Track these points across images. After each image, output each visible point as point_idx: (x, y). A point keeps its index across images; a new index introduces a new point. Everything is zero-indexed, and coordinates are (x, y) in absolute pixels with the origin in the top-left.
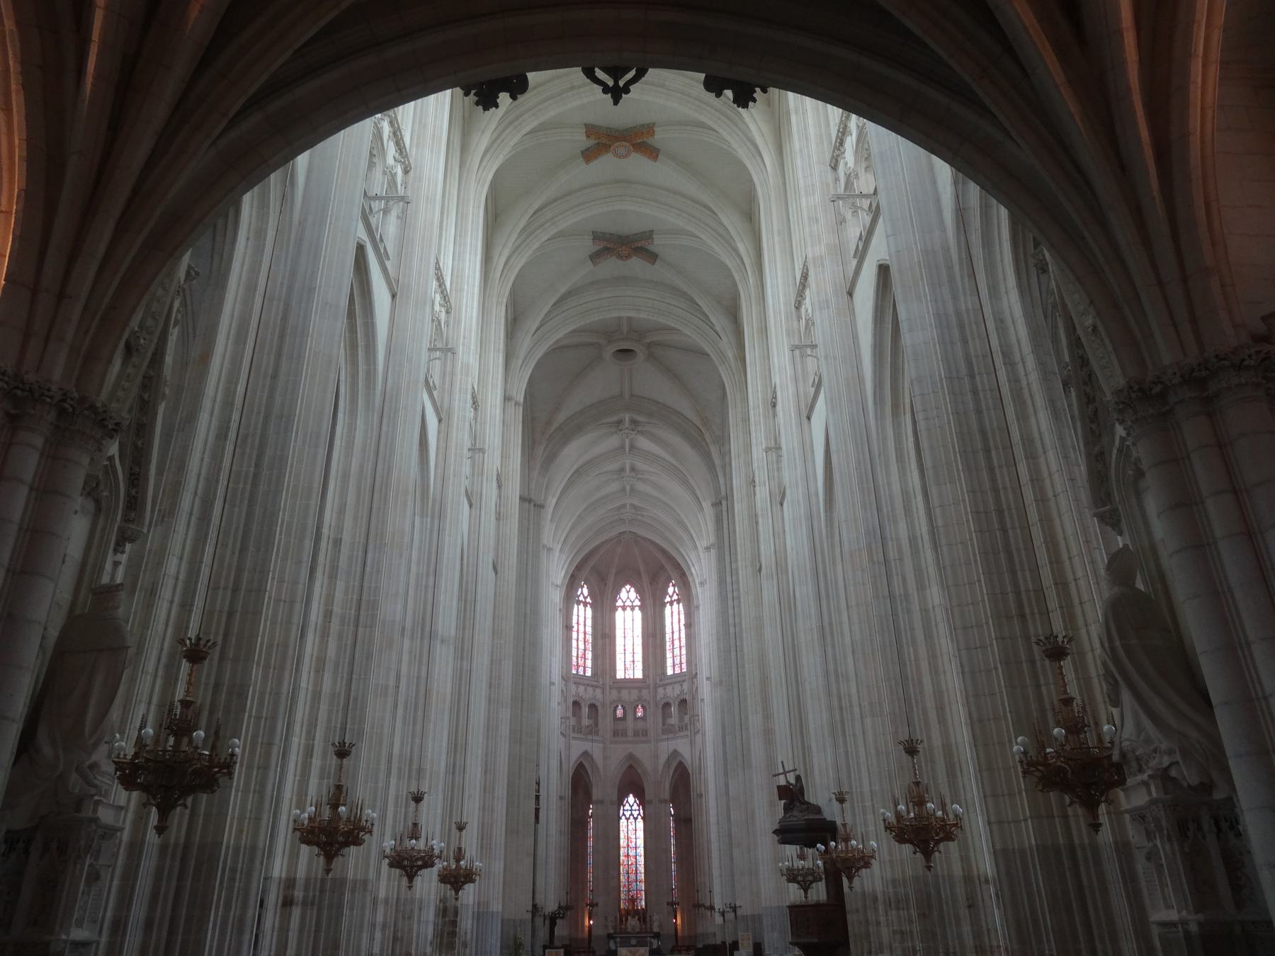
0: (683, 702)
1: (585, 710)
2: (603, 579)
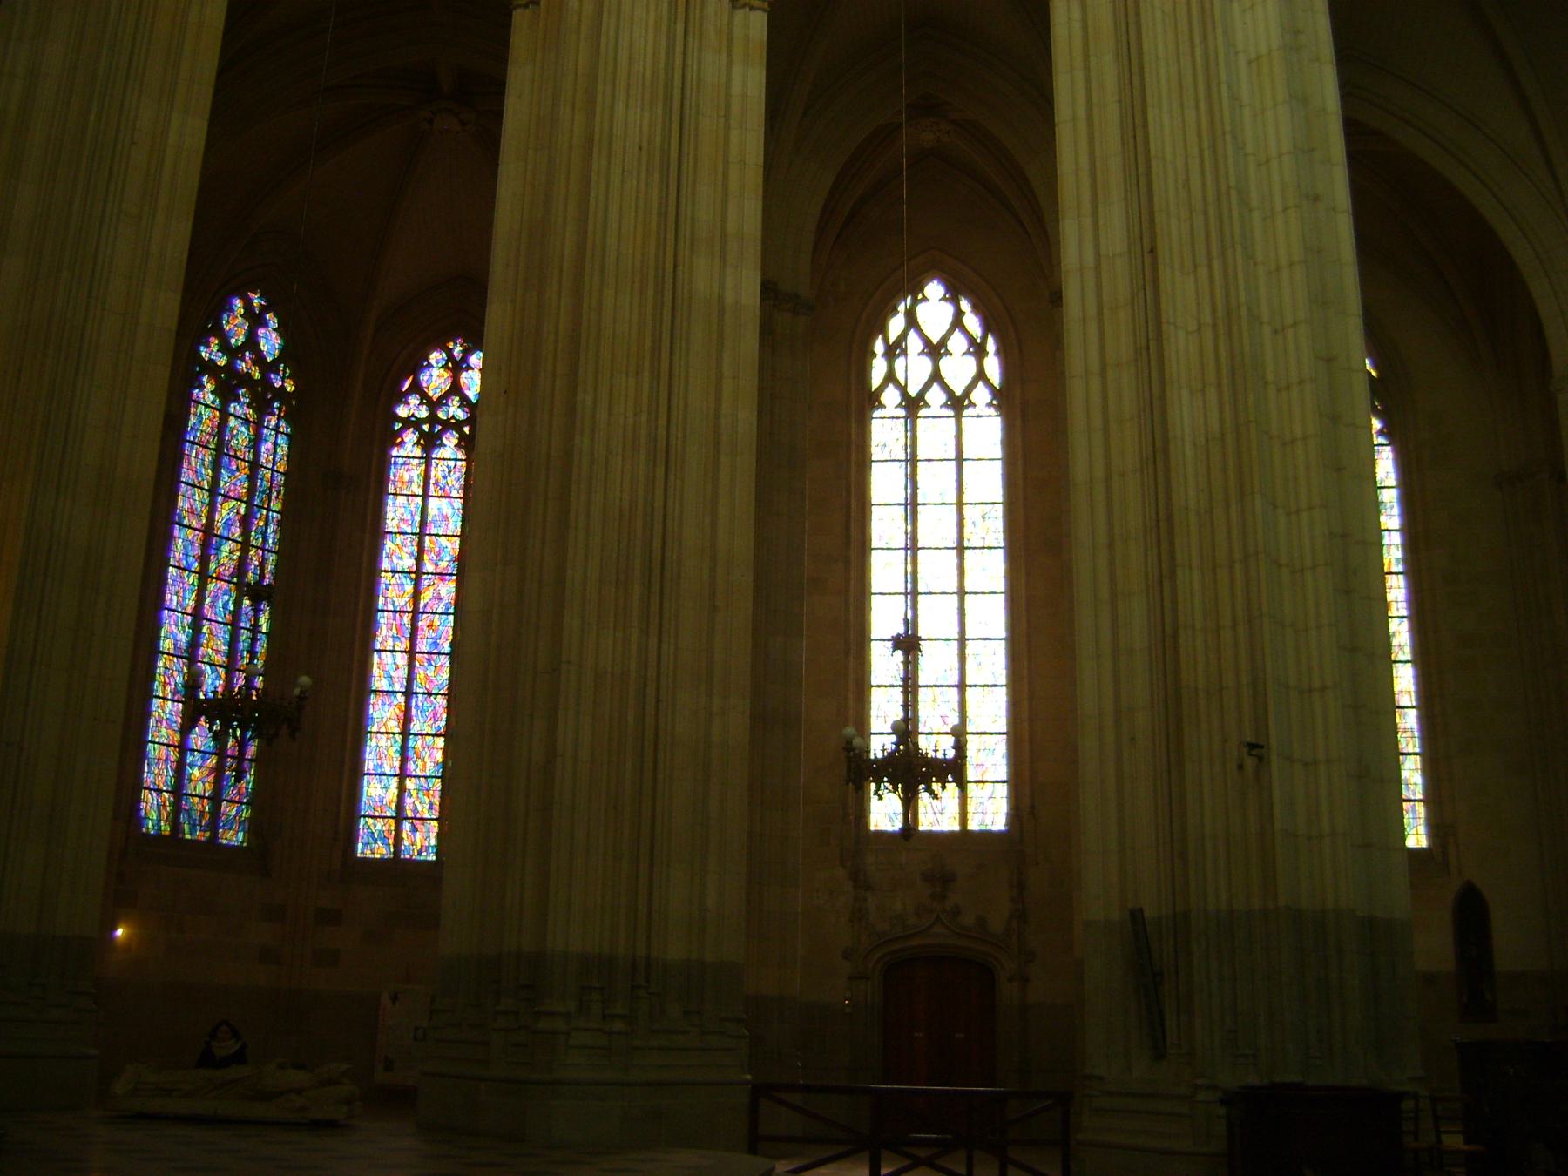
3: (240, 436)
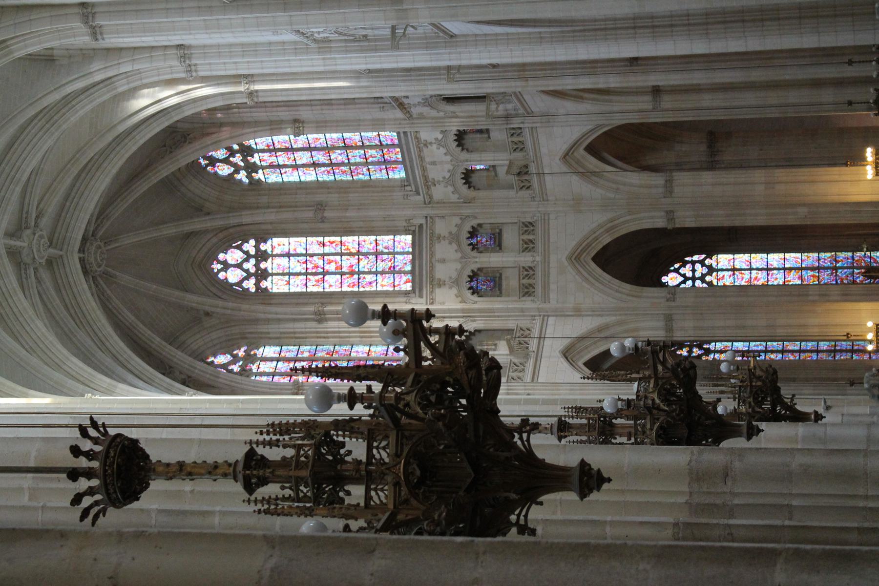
2: (197, 318)
3: (266, 367)
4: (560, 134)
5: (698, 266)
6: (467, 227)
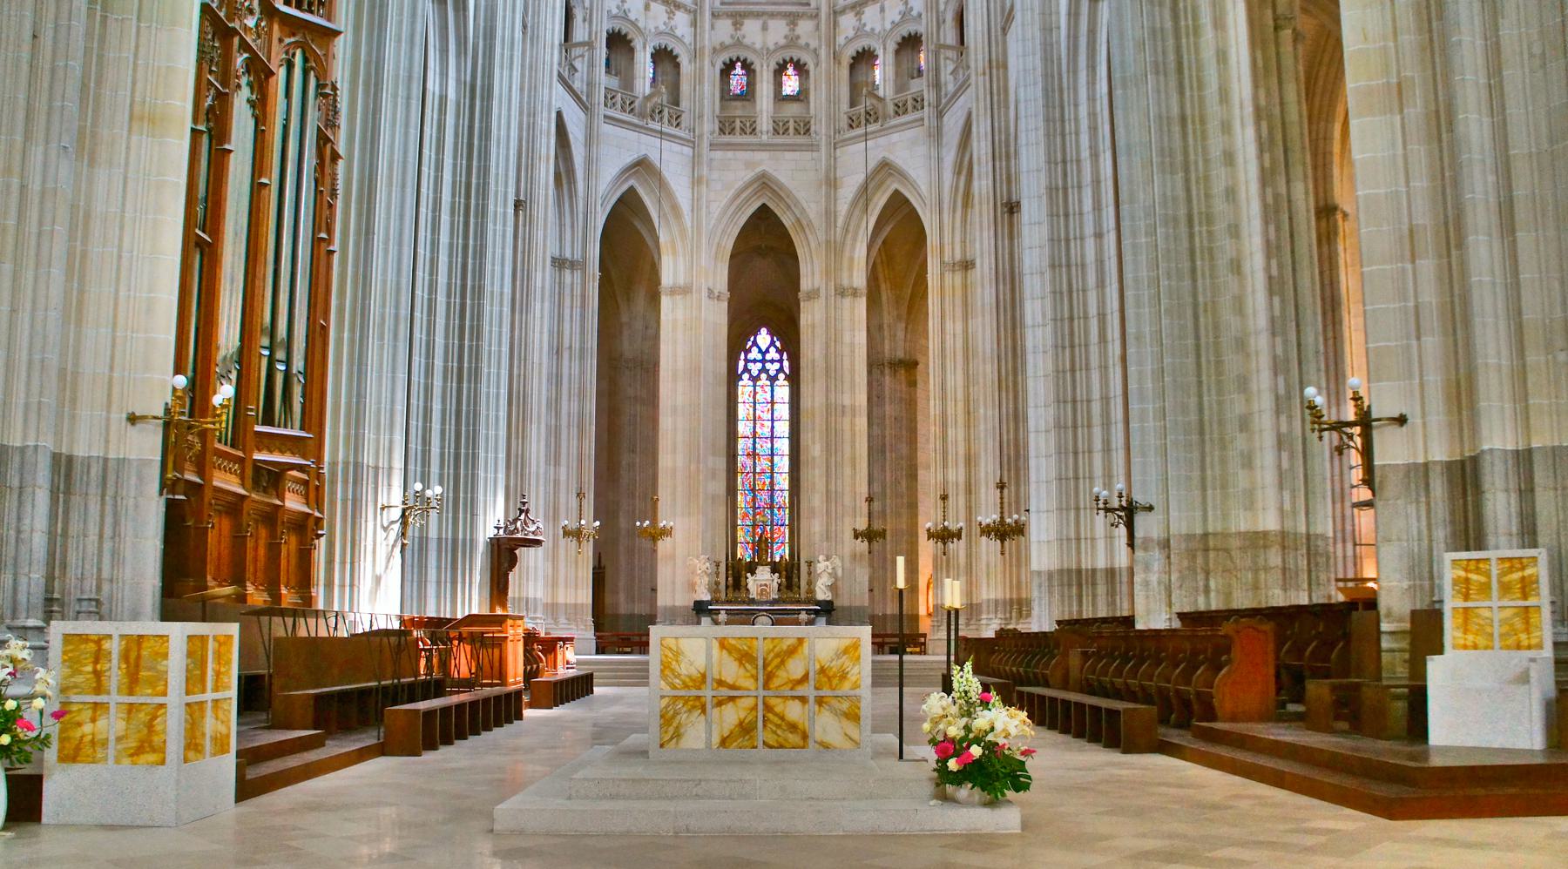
0: (910, 43)
1: (644, 66)
4: (912, 155)
5: (777, 366)
6: (806, 58)
